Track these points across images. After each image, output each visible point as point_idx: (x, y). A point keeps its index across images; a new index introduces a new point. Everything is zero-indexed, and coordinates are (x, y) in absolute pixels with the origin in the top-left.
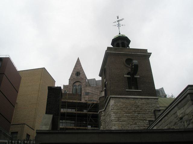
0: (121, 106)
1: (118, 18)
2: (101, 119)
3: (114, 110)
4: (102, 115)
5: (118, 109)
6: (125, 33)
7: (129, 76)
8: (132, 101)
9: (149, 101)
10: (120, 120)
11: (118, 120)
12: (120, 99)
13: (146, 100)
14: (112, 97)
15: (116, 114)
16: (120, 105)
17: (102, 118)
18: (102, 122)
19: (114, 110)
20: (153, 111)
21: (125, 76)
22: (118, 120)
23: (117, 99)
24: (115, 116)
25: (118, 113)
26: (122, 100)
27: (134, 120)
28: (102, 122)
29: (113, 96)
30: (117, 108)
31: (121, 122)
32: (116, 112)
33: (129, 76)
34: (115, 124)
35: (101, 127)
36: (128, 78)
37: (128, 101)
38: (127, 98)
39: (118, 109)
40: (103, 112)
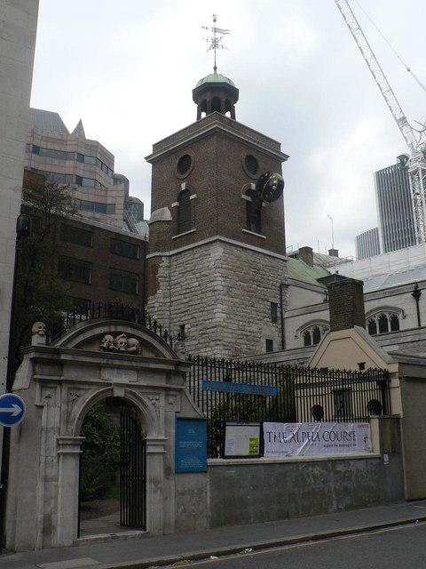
1: (215, 21)
3: (222, 271)
6: (230, 72)
7: (249, 199)
8: (251, 257)
9: (274, 263)
11: (228, 294)
12: (233, 247)
13: (271, 259)
14: (221, 241)
17: (161, 272)
19: (222, 271)
20: (278, 285)
21: (244, 196)
22: (228, 294)
23: (228, 247)
26: (235, 250)
27: (251, 297)
29: (223, 239)
33: (249, 199)
36: (247, 201)
37: (244, 255)
38: (243, 248)
40: (163, 259)
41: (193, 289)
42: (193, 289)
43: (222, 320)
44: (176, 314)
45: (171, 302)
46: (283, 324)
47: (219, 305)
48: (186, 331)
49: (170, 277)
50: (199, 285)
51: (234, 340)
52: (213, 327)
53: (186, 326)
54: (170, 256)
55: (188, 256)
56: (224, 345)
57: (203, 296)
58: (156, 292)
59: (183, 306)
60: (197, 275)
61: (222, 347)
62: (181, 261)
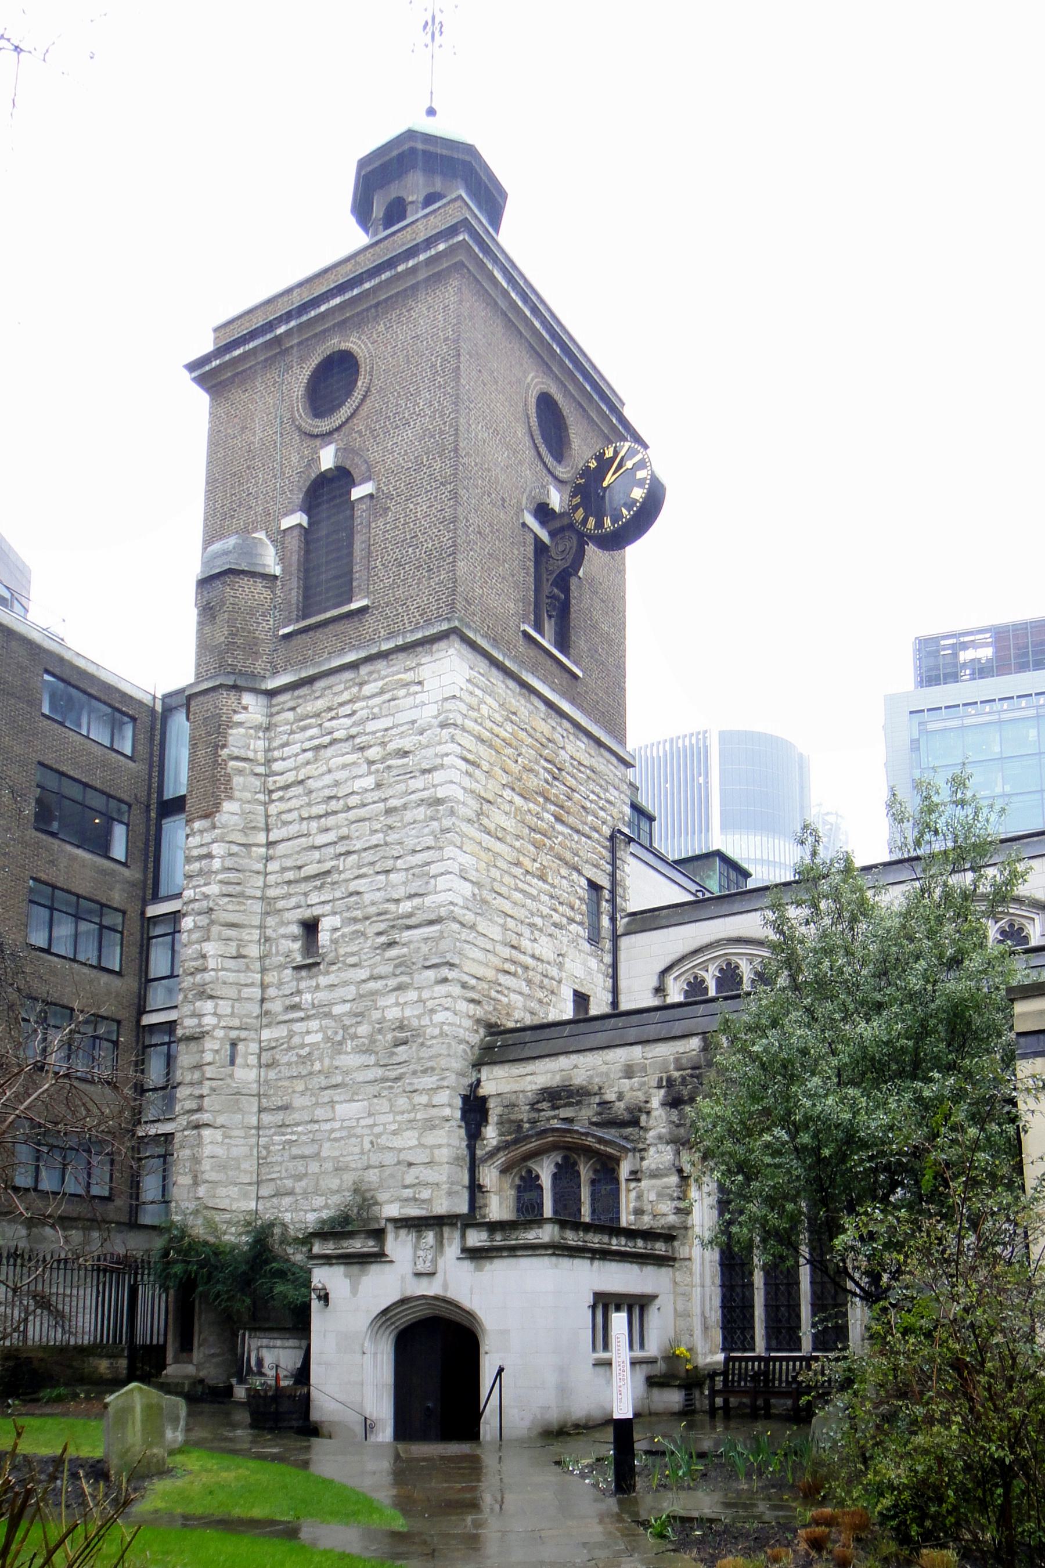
0: (495, 727)
2: (236, 752)
4: (237, 718)
5: (483, 741)
10: (485, 821)
12: (494, 671)
15: (470, 769)
16: (489, 717)
18: (240, 772)
24: (466, 782)
25: (478, 766)
28: (240, 772)
30: (478, 728)
31: (489, 834)
32: (470, 757)
34: (463, 835)
35: (227, 806)
39: (483, 741)
41: (353, 801)
42: (353, 801)
43: (460, 901)
44: (289, 882)
45: (270, 844)
46: (615, 951)
47: (450, 851)
48: (324, 937)
49: (268, 762)
50: (379, 786)
51: (490, 974)
52: (431, 923)
53: (325, 924)
54: (271, 694)
55: (341, 688)
56: (464, 986)
57: (390, 821)
58: (217, 807)
59: (316, 855)
60: (373, 753)
61: (457, 990)
62: (310, 707)
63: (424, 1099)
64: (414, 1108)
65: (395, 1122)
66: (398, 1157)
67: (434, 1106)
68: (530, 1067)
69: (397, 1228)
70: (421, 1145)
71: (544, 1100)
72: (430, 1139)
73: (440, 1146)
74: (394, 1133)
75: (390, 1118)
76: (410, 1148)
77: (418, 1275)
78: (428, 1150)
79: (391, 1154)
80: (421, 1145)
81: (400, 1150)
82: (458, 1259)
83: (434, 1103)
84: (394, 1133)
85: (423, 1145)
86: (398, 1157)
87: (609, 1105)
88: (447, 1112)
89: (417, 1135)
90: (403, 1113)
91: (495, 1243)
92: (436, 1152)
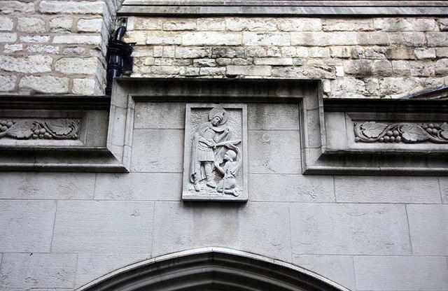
63: (67, 23)
64: (50, 32)
65: (18, 42)
66: (18, 83)
67: (79, 32)
68: (189, 24)
69: (138, 100)
70: (54, 72)
71: (206, 57)
72: (71, 66)
73: (85, 76)
74: (15, 55)
75: (14, 37)
76: (38, 75)
77: (192, 205)
78: (66, 80)
79: (8, 79)
80: (54, 72)
81: (22, 75)
82: (309, 173)
83: (80, 29)
84: (15, 55)
85: (61, 74)
86: (18, 83)
87: (286, 68)
88: (97, 40)
89: (50, 60)
90: (33, 34)
91: (401, 146)
92: (77, 81)
